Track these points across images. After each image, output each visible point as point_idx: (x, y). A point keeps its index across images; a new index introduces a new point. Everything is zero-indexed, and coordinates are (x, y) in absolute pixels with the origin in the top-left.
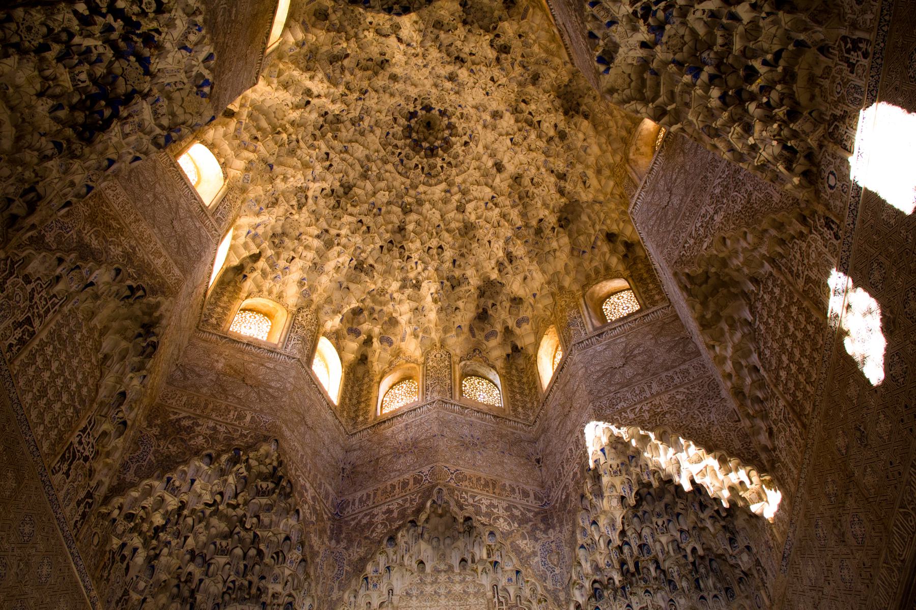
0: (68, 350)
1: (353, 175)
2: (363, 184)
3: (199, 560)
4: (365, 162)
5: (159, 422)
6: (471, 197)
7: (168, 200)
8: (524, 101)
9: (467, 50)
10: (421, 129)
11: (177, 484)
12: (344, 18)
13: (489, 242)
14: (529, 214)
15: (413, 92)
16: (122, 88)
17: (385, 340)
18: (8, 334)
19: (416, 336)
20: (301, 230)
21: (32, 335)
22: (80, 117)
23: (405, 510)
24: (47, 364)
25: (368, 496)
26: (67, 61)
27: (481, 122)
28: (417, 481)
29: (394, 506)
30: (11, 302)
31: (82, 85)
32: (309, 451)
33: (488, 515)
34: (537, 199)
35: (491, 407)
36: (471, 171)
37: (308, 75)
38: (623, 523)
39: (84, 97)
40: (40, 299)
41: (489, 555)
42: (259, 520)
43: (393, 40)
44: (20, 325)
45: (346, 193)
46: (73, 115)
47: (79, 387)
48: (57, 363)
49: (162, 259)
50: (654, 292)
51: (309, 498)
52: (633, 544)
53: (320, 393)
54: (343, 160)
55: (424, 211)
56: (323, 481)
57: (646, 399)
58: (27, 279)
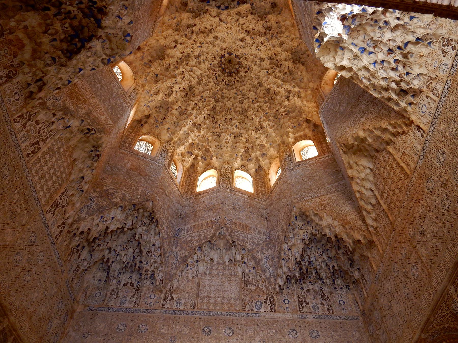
0: (57, 156)
1: (194, 82)
3: (113, 253)
5: (99, 190)
6: (246, 97)
7: (107, 88)
8: (275, 54)
9: (251, 27)
10: (227, 63)
11: (105, 219)
12: (195, 6)
13: (253, 118)
14: (272, 107)
15: (224, 45)
16: (86, 33)
17: (204, 158)
18: (27, 149)
19: (217, 158)
20: (169, 106)
21: (39, 149)
23: (207, 235)
24: (46, 163)
25: (191, 227)
26: (58, 17)
27: (254, 62)
28: (213, 223)
30: (29, 134)
31: (66, 30)
32: (166, 206)
33: (243, 241)
34: (276, 101)
35: (247, 192)
36: (247, 85)
37: (176, 33)
38: (302, 251)
39: (67, 35)
40: (44, 132)
43: (217, 19)
44: (33, 144)
45: (190, 91)
46: (61, 45)
47: (62, 174)
49: (104, 117)
50: (325, 148)
51: (165, 227)
52: (306, 261)
54: (190, 75)
55: (225, 102)
57: (318, 197)
58: (37, 123)
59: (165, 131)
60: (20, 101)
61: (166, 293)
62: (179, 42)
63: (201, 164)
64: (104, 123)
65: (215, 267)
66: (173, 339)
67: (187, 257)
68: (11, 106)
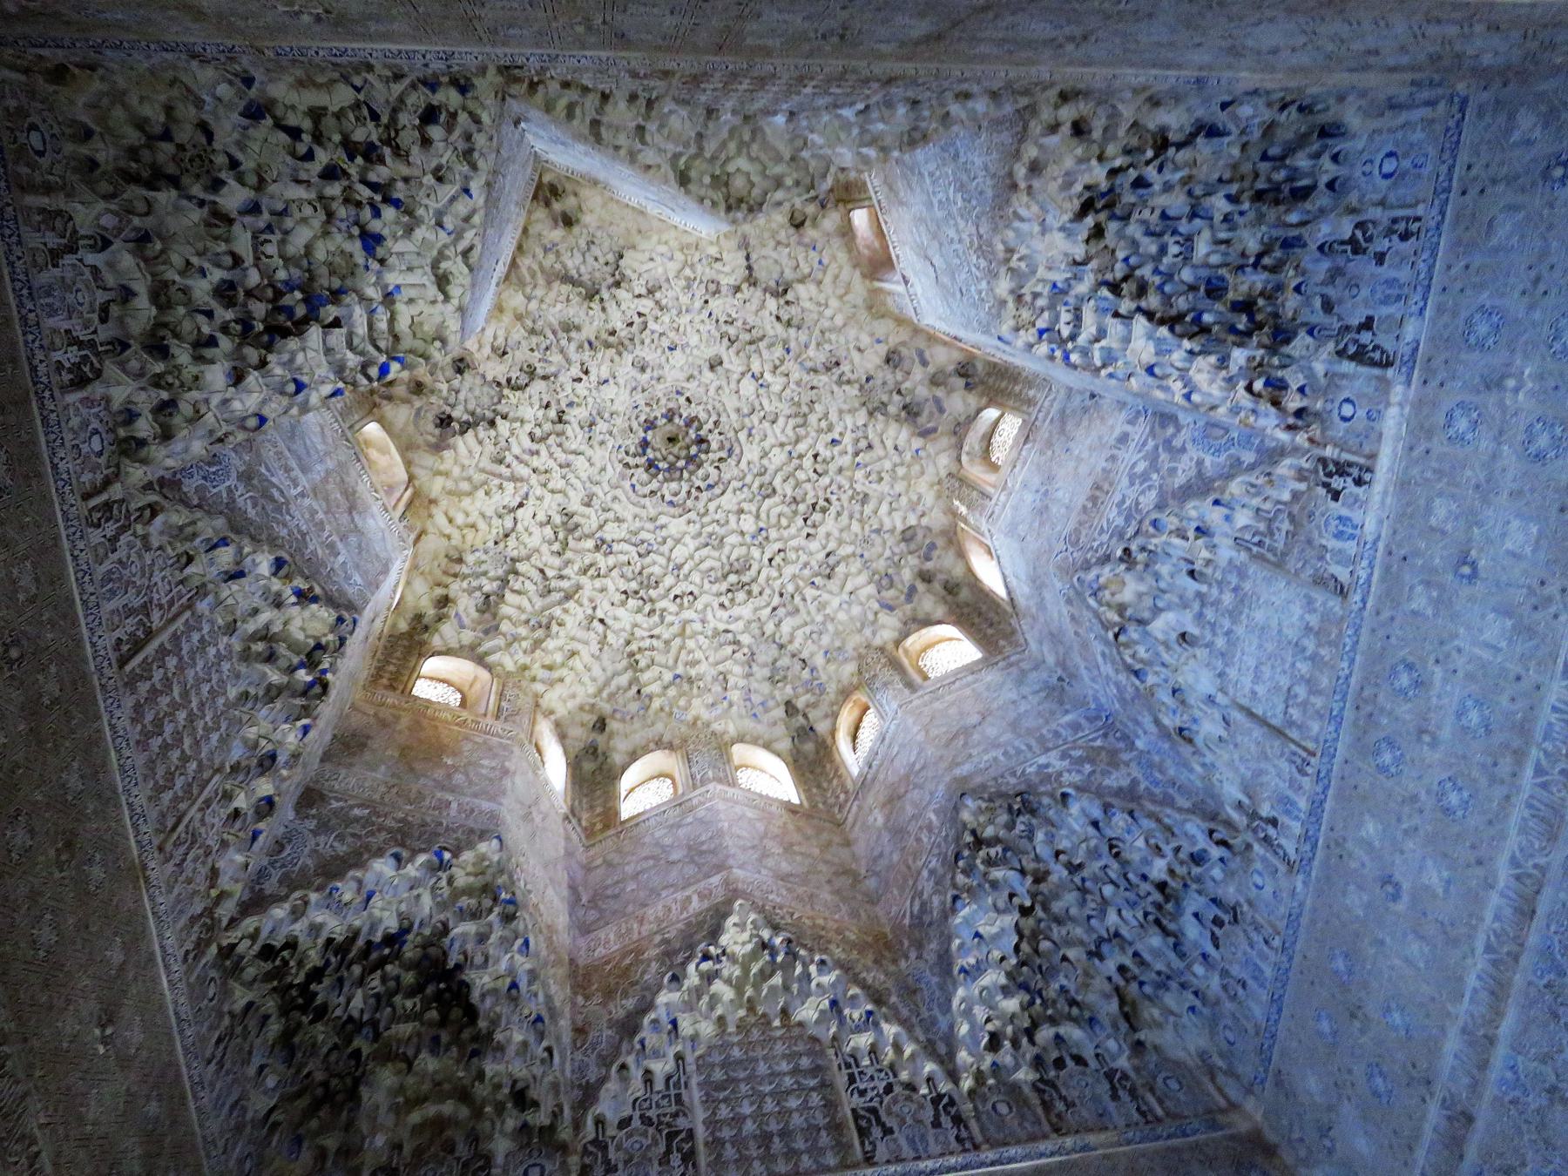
4: (702, 540)
5: (906, 943)
7: (646, 858)
9: (541, 413)
10: (675, 450)
12: (491, 574)
14: (771, 333)
19: (923, 515)
21: (691, 1134)
22: (456, 1013)
24: (738, 1120)
28: (1069, 602)
29: (1098, 647)
33: (1128, 519)
36: (725, 400)
37: (555, 628)
38: (1162, 322)
41: (1186, 538)
43: (520, 512)
44: (668, 1151)
45: (737, 572)
47: (796, 1071)
48: (746, 1102)
49: (695, 898)
54: (687, 576)
56: (1054, 726)
58: (624, 1123)
59: (832, 668)
61: (1255, 831)
62: (590, 611)
63: (945, 561)
64: (706, 904)
65: (1209, 637)
66: (1390, 889)
67: (1157, 722)
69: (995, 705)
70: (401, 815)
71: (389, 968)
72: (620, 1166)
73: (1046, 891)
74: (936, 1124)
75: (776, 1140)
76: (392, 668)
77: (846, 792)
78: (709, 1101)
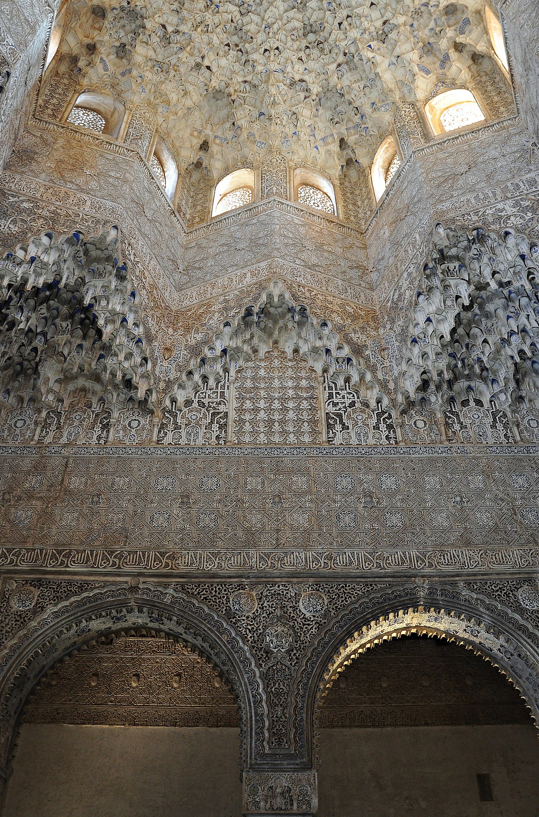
2: (310, 10)
3: (513, 338)
11: (422, 336)
12: (128, 28)
21: (226, 415)
22: (92, 332)
24: (256, 410)
37: (172, 73)
39: (79, 326)
42: (498, 273)
44: (212, 422)
47: (297, 388)
48: (262, 402)
49: (249, 275)
53: (457, 138)
56: (517, 181)
58: (188, 403)
60: (142, 422)
62: (199, 60)
68: (139, 439)
69: (481, 160)
70: (53, 208)
71: (51, 302)
72: (183, 426)
73: (484, 297)
74: (377, 428)
75: (276, 424)
76: (55, 101)
77: (371, 211)
78: (241, 398)
